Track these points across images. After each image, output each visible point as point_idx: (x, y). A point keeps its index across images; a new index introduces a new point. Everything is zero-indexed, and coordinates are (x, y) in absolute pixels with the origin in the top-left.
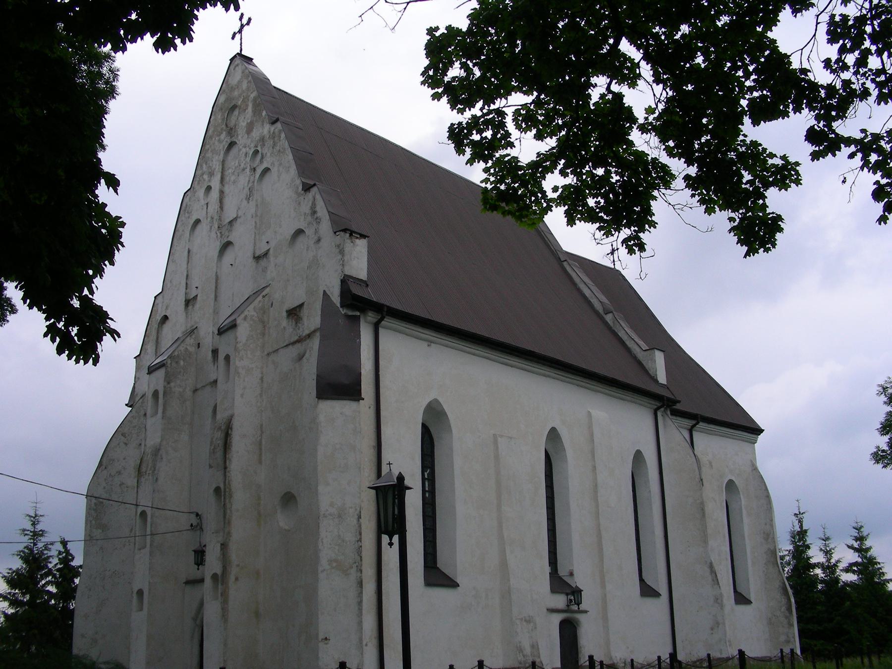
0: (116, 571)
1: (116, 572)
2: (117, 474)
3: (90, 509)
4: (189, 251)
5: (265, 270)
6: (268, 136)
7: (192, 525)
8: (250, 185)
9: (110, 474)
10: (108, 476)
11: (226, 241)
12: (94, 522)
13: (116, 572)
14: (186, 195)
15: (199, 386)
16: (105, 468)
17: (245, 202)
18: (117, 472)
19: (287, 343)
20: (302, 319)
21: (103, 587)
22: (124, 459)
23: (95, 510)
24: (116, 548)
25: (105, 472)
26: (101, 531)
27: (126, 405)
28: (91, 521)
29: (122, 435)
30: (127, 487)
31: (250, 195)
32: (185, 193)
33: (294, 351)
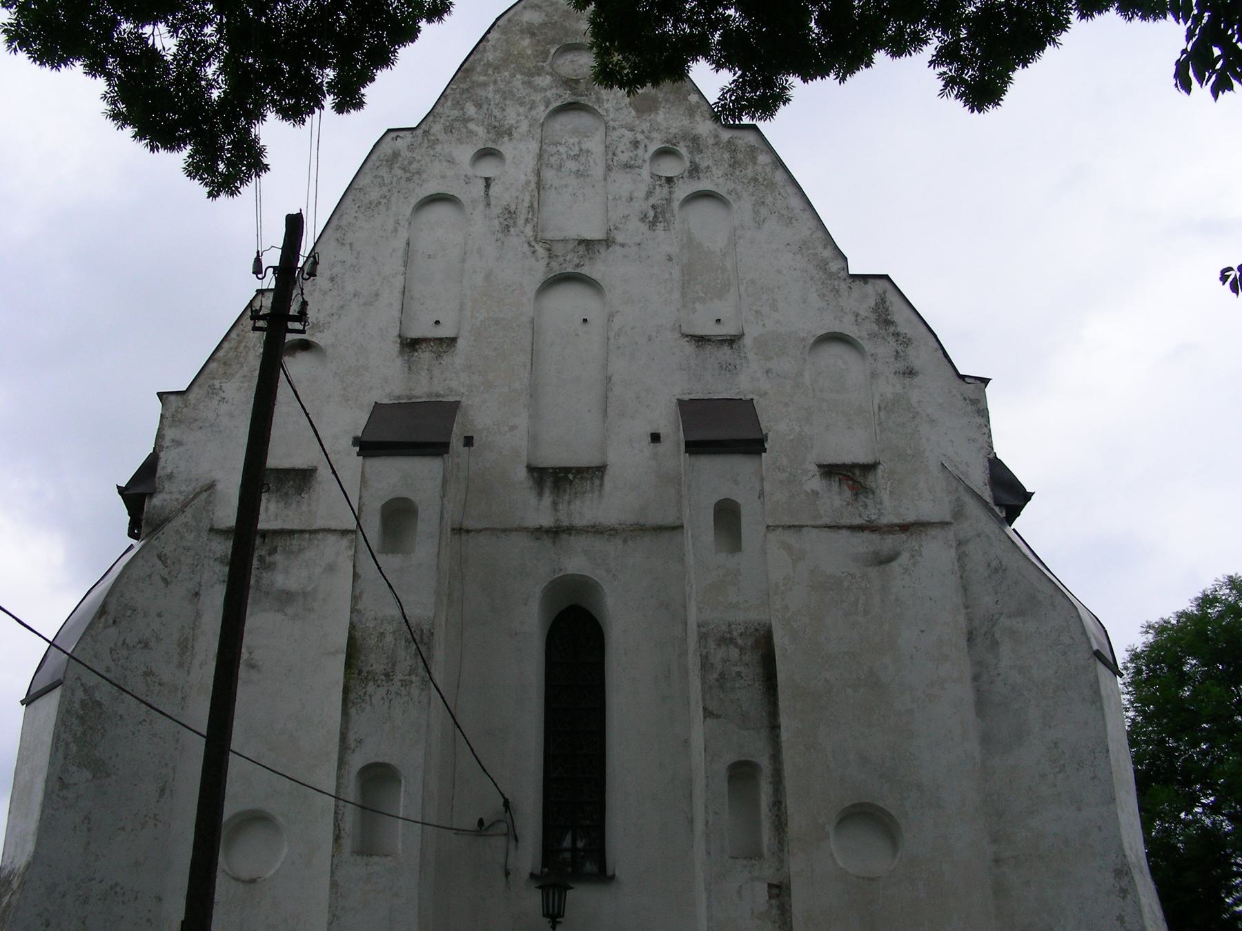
0: (117, 884)
1: (118, 889)
2: (139, 645)
3: (68, 711)
4: (408, 244)
5: (729, 369)
6: (711, 141)
7: (481, 822)
8: (652, 201)
9: (124, 641)
10: (120, 643)
11: (569, 270)
12: (74, 748)
13: (118, 889)
14: (394, 134)
15: (468, 524)
16: (114, 622)
17: (634, 229)
18: (140, 642)
19: (826, 520)
20: (873, 493)
21: (84, 922)
22: (159, 615)
23: (82, 719)
24: (123, 829)
25: (112, 631)
26: (90, 777)
27: (118, 487)
28: (67, 744)
29: (159, 557)
30: (160, 684)
31: (655, 216)
32: (389, 131)
33: (863, 544)
